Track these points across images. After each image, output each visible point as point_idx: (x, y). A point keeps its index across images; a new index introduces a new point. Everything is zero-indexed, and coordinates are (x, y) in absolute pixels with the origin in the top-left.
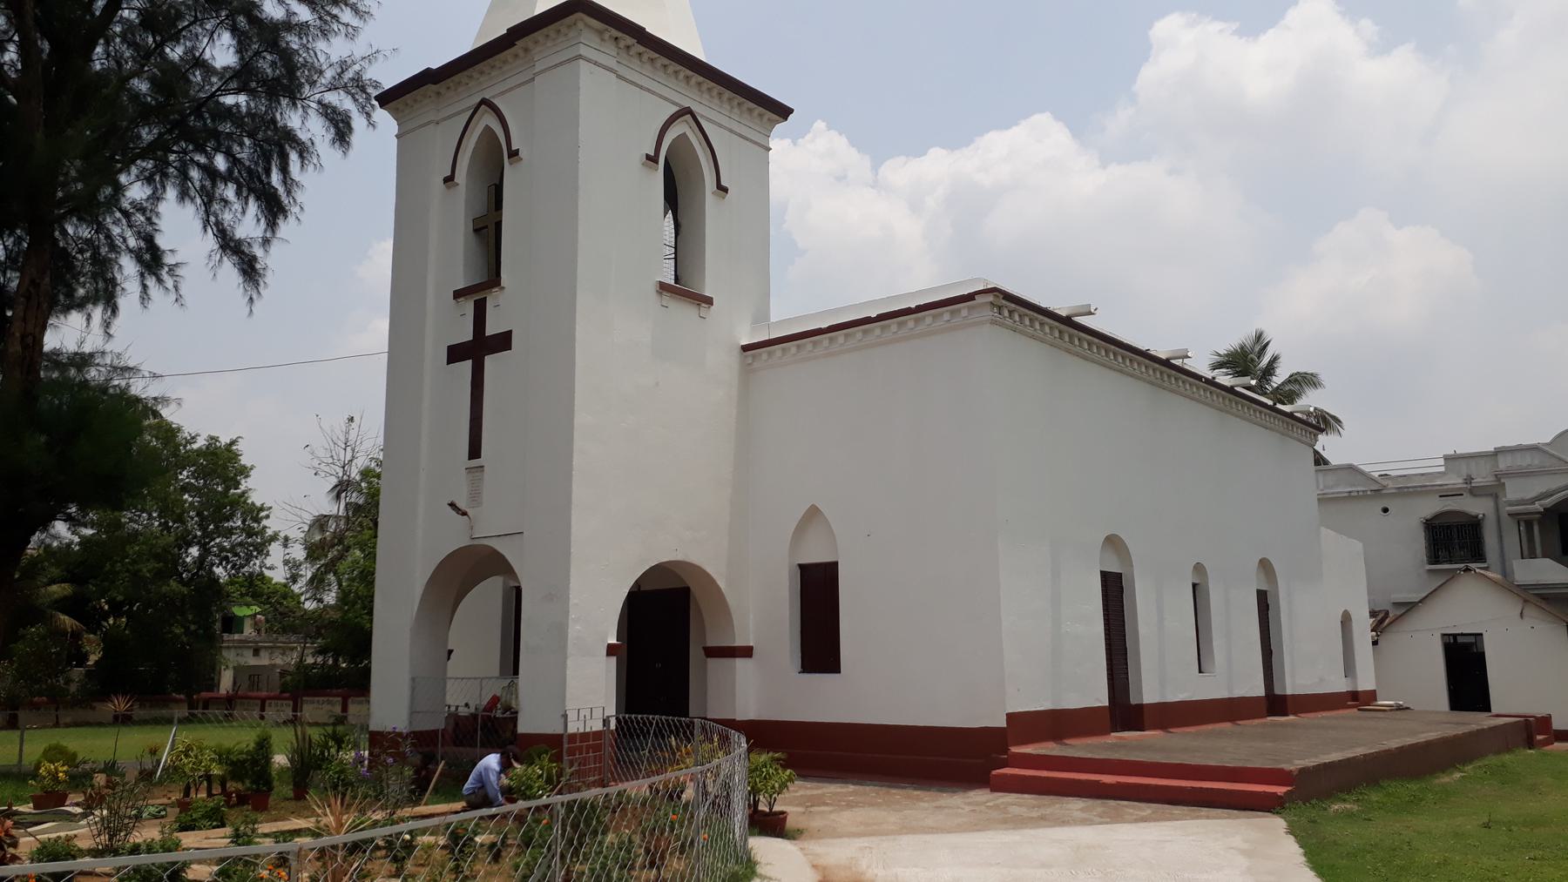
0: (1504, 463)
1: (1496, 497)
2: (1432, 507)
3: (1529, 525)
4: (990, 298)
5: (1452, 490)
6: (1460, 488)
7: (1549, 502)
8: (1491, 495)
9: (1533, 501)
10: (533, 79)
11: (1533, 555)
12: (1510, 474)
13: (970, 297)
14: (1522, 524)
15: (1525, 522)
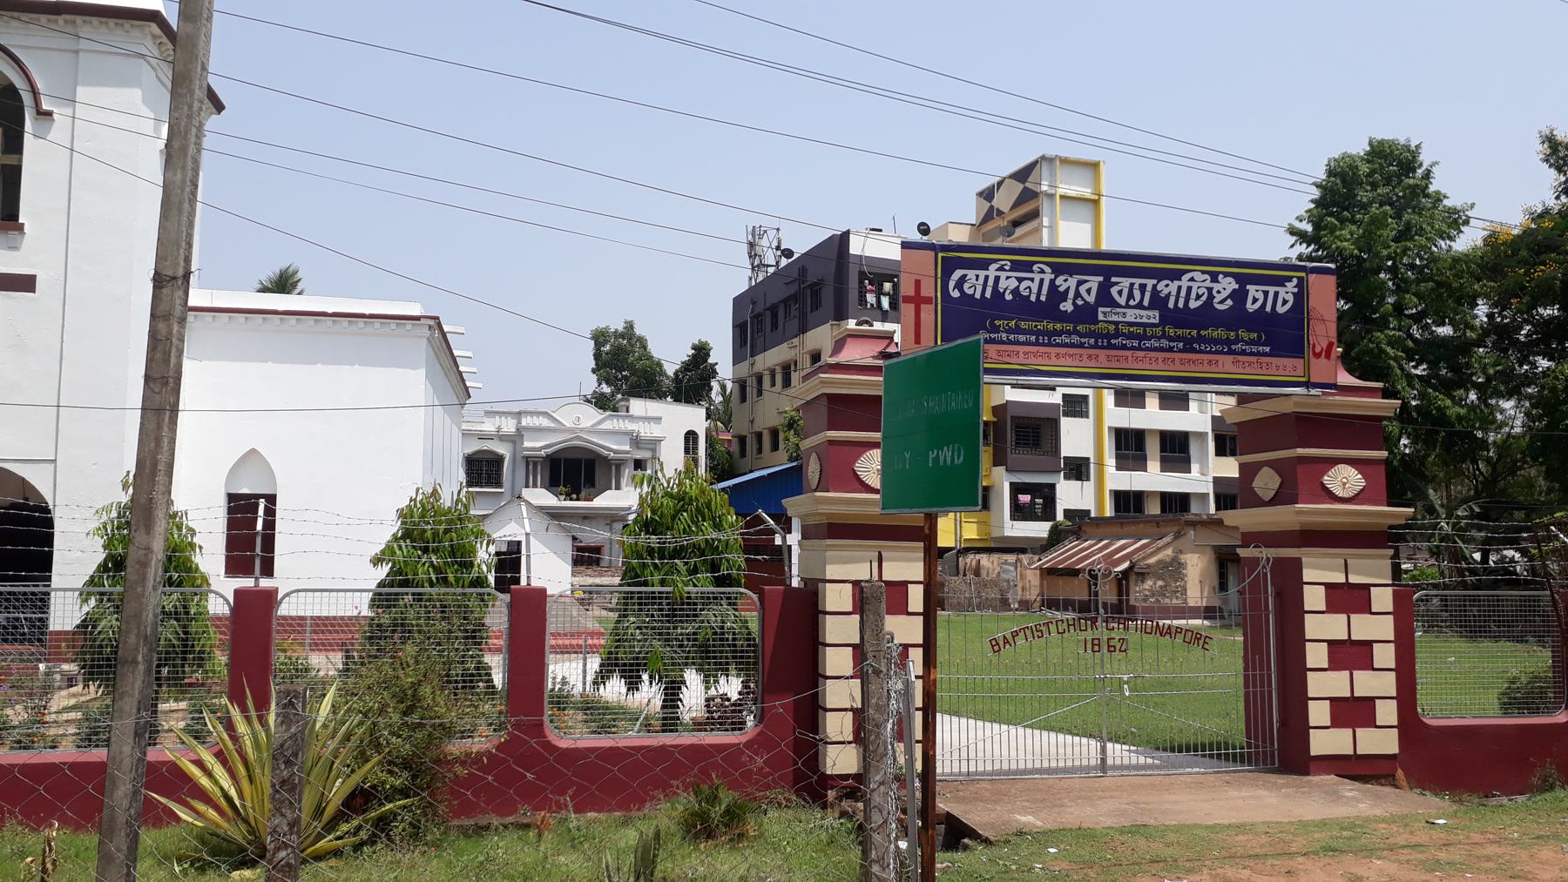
0: (526, 421)
1: (514, 442)
2: (474, 446)
3: (535, 464)
4: (432, 322)
5: (488, 435)
6: (492, 435)
7: (550, 451)
8: (512, 441)
9: (540, 449)
10: (77, 52)
11: (535, 486)
12: (527, 429)
13: (417, 318)
14: (531, 464)
15: (530, 462)
